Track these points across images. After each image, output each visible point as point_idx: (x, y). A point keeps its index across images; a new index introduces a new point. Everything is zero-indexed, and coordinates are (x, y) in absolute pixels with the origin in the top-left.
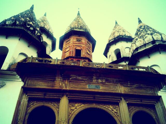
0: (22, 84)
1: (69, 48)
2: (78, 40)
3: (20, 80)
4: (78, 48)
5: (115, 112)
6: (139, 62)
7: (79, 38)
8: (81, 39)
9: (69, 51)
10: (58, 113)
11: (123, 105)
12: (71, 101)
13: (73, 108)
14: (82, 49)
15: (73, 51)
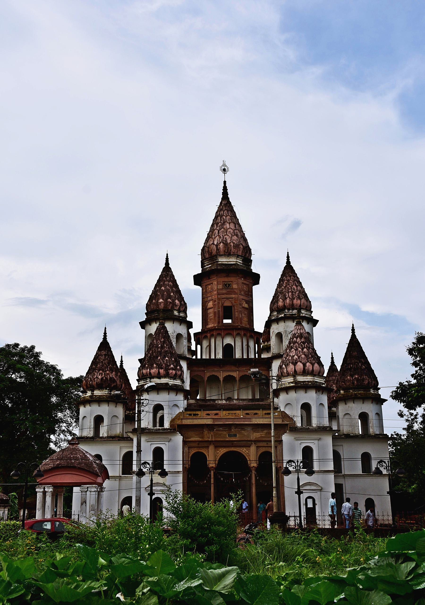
0: (182, 437)
1: (211, 301)
2: (226, 285)
3: (180, 435)
4: (227, 304)
5: (247, 453)
6: (280, 395)
7: (226, 279)
8: (232, 282)
9: (212, 308)
10: (209, 456)
11: (253, 449)
12: (216, 447)
13: (219, 452)
14: (234, 306)
15: (219, 311)
